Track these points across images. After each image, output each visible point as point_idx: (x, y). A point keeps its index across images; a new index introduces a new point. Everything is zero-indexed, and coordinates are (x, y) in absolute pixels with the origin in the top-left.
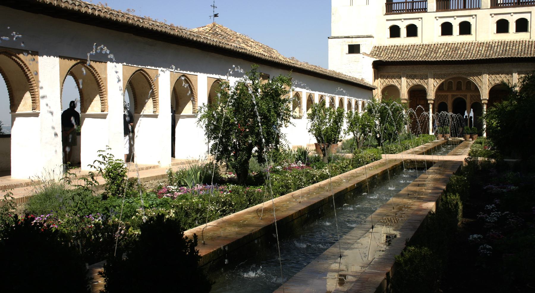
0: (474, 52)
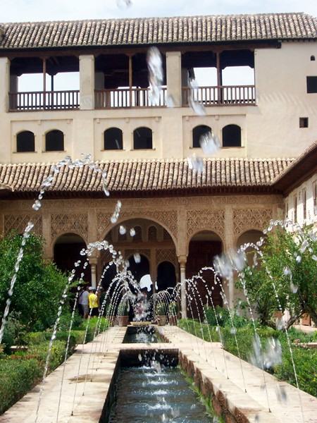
0: (161, 178)
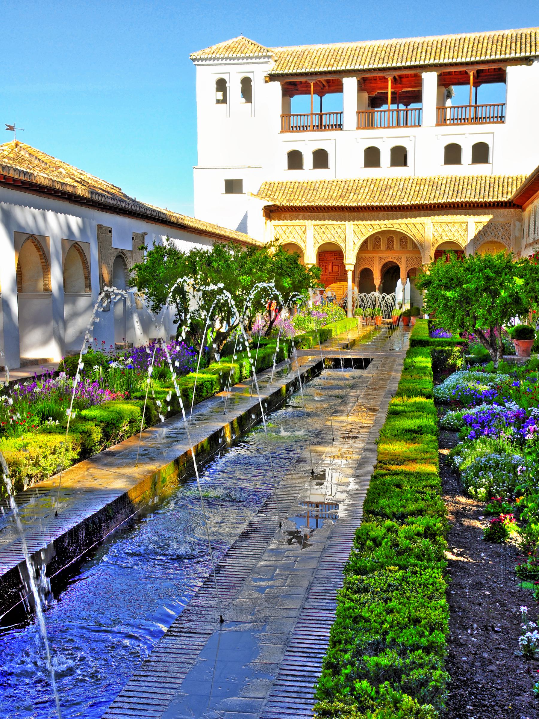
0: (412, 193)
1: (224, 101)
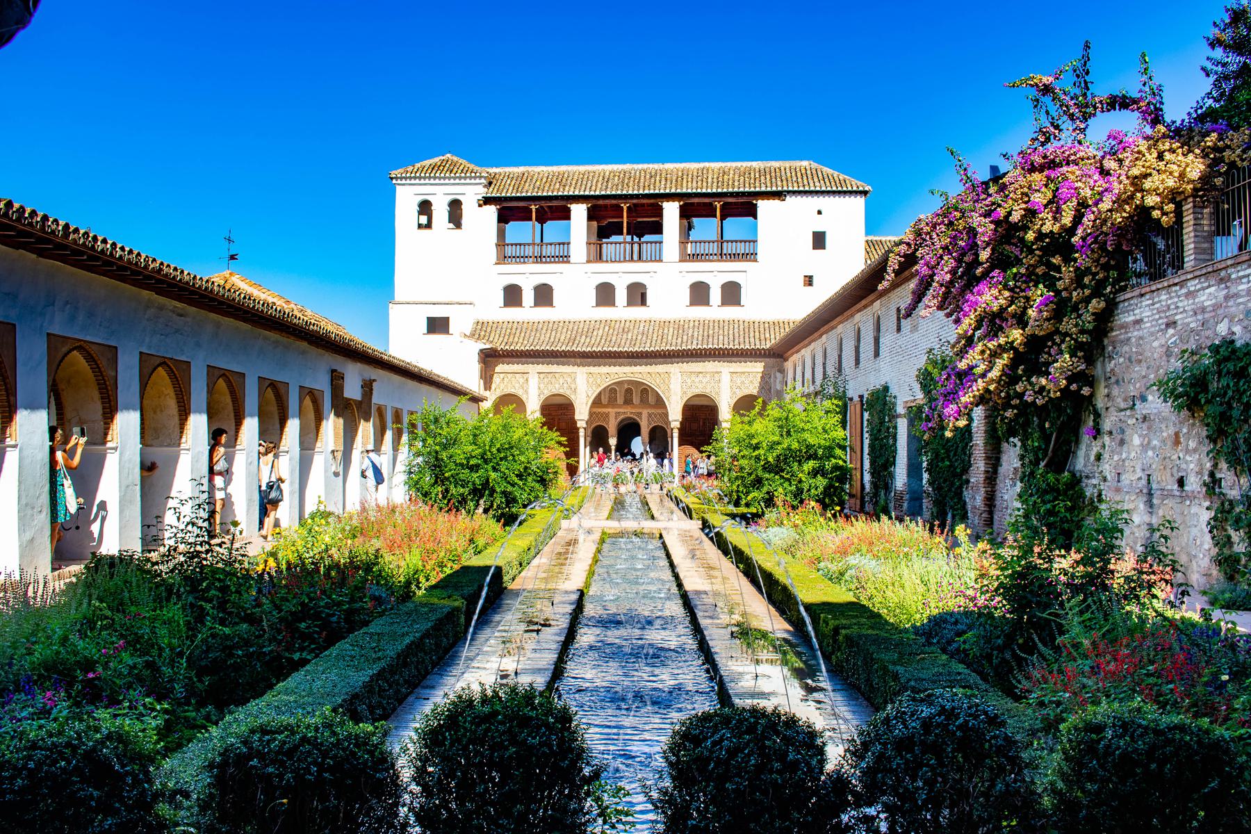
1: (429, 226)
